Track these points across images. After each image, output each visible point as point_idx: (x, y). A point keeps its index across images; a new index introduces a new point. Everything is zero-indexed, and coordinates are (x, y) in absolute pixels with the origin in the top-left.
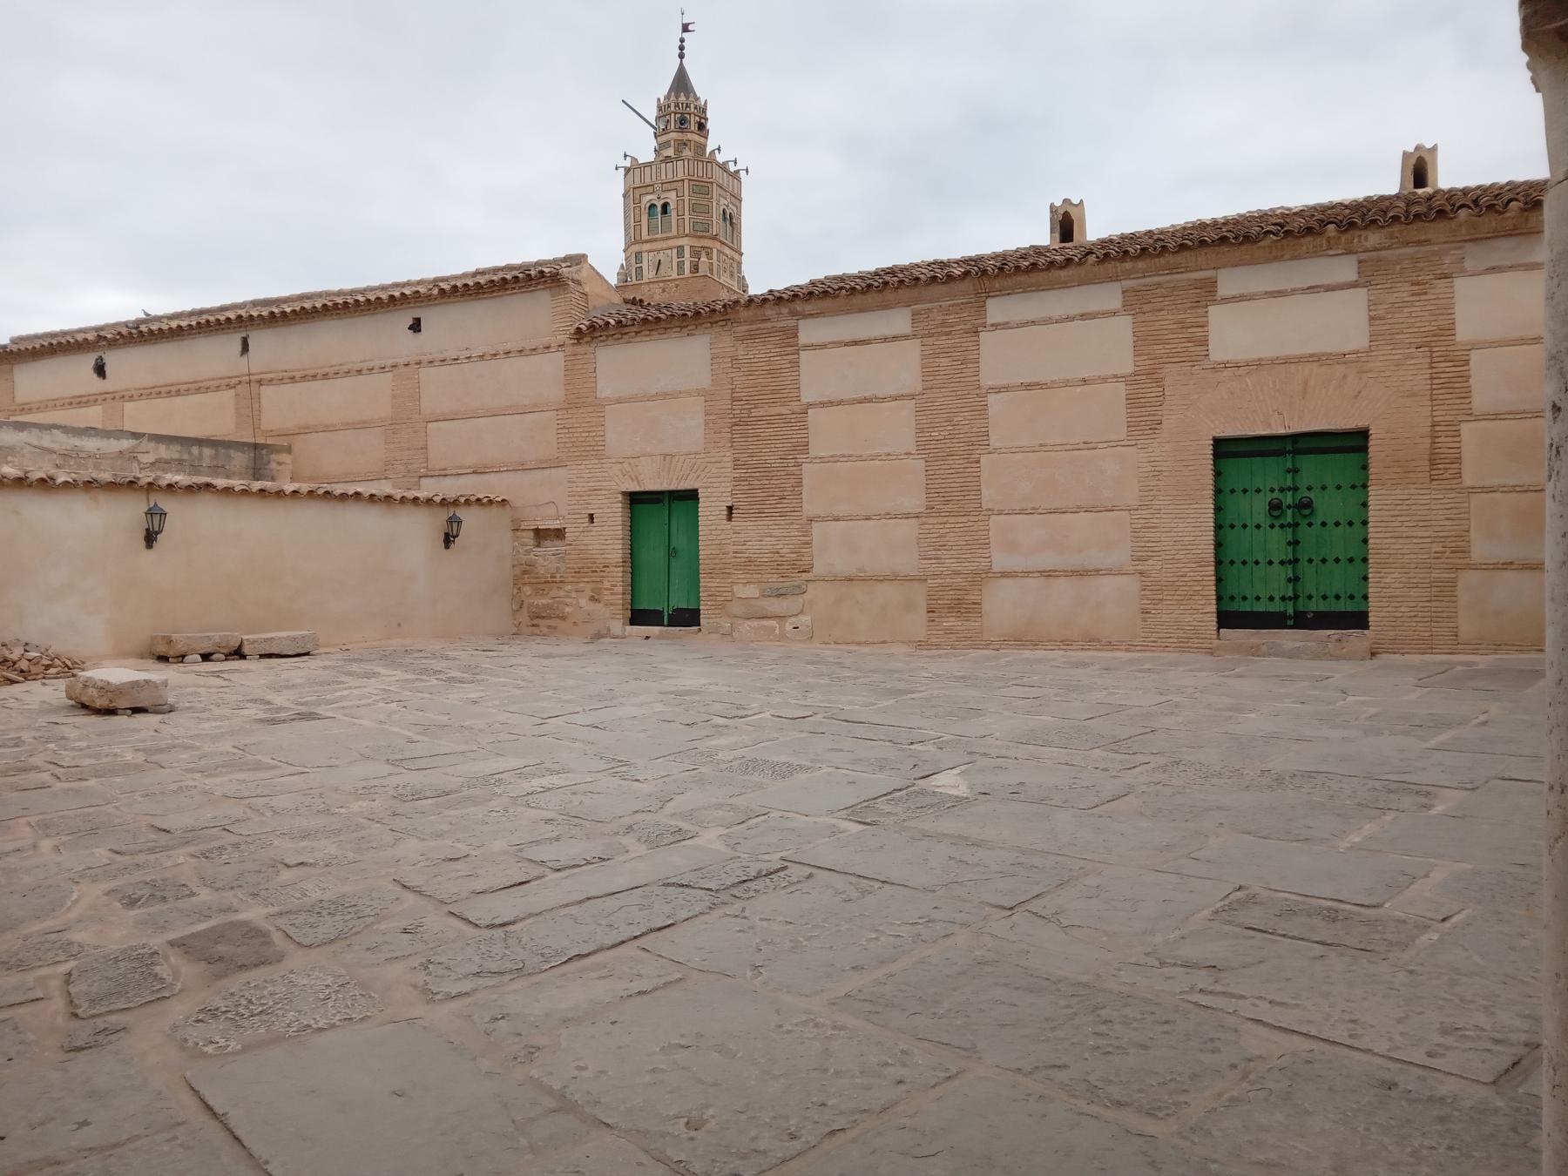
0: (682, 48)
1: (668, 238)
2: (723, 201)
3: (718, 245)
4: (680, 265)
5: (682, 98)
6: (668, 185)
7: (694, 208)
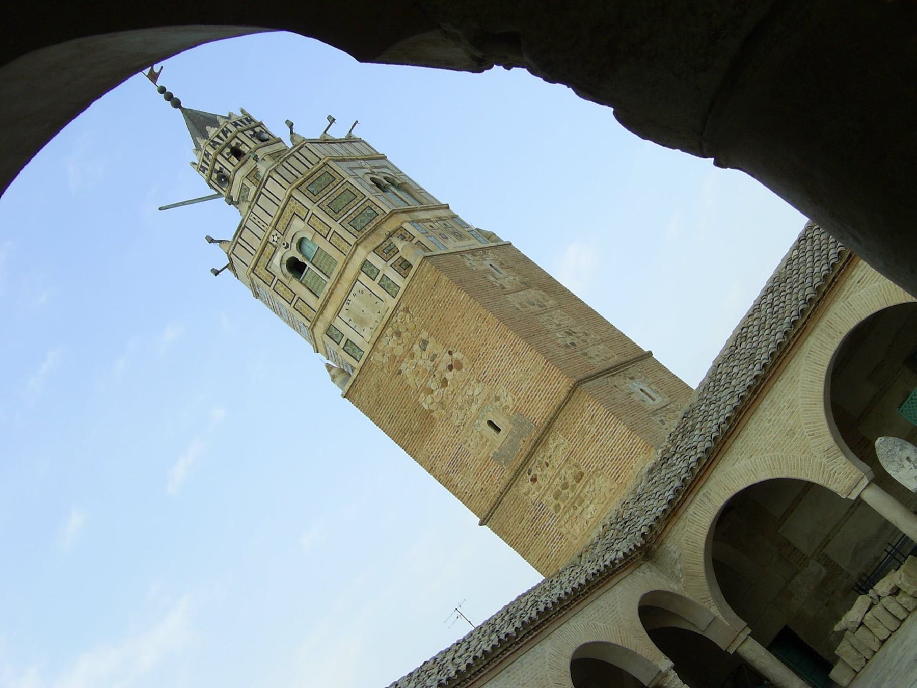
0: (169, 97)
1: (341, 275)
3: (404, 217)
5: (212, 131)
6: (280, 224)
7: (334, 211)
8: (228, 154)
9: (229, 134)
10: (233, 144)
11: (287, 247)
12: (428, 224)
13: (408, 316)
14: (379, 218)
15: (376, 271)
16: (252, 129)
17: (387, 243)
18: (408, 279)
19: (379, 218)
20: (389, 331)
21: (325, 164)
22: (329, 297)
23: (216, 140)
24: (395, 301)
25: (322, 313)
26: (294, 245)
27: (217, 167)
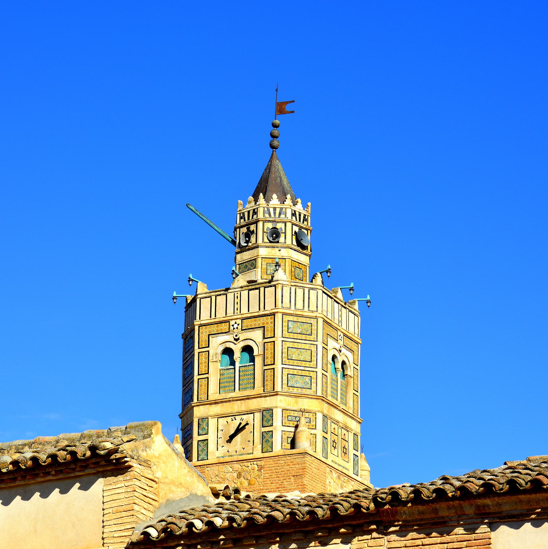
1: (248, 398)
2: (332, 343)
4: (267, 439)
5: (275, 201)
8: (268, 228)
9: (283, 216)
10: (279, 226)
11: (235, 339)
12: (333, 426)
13: (257, 473)
14: (308, 392)
15: (270, 423)
16: (301, 228)
17: (296, 414)
18: (281, 453)
19: (308, 392)
20: (237, 466)
21: (316, 318)
22: (226, 402)
23: (272, 210)
24: (262, 455)
25: (210, 404)
26: (242, 344)
27: (253, 227)
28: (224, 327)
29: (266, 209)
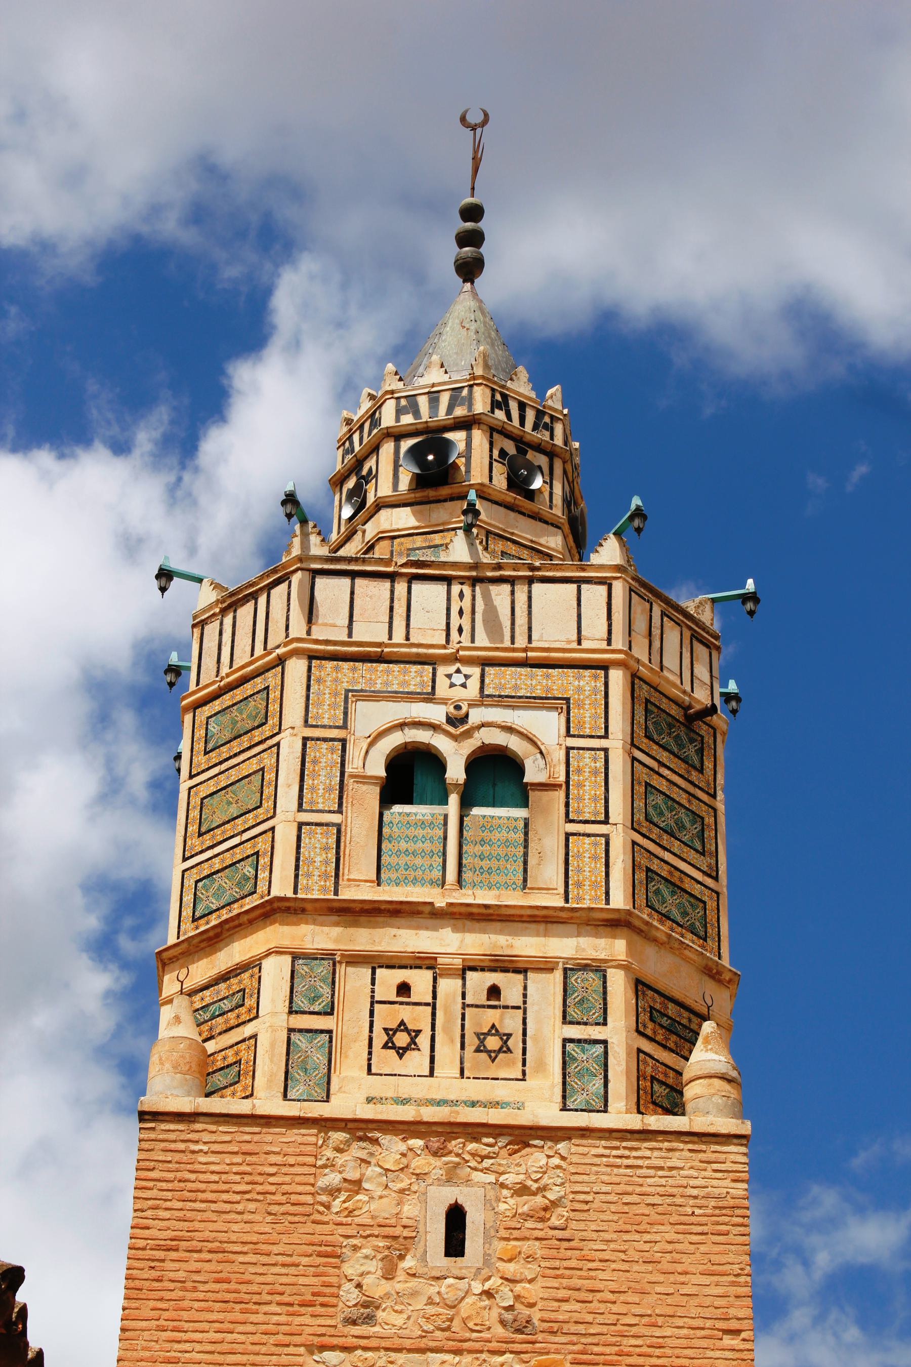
8: (503, 454)
23: (514, 407)
28: (415, 677)
29: (498, 397)
